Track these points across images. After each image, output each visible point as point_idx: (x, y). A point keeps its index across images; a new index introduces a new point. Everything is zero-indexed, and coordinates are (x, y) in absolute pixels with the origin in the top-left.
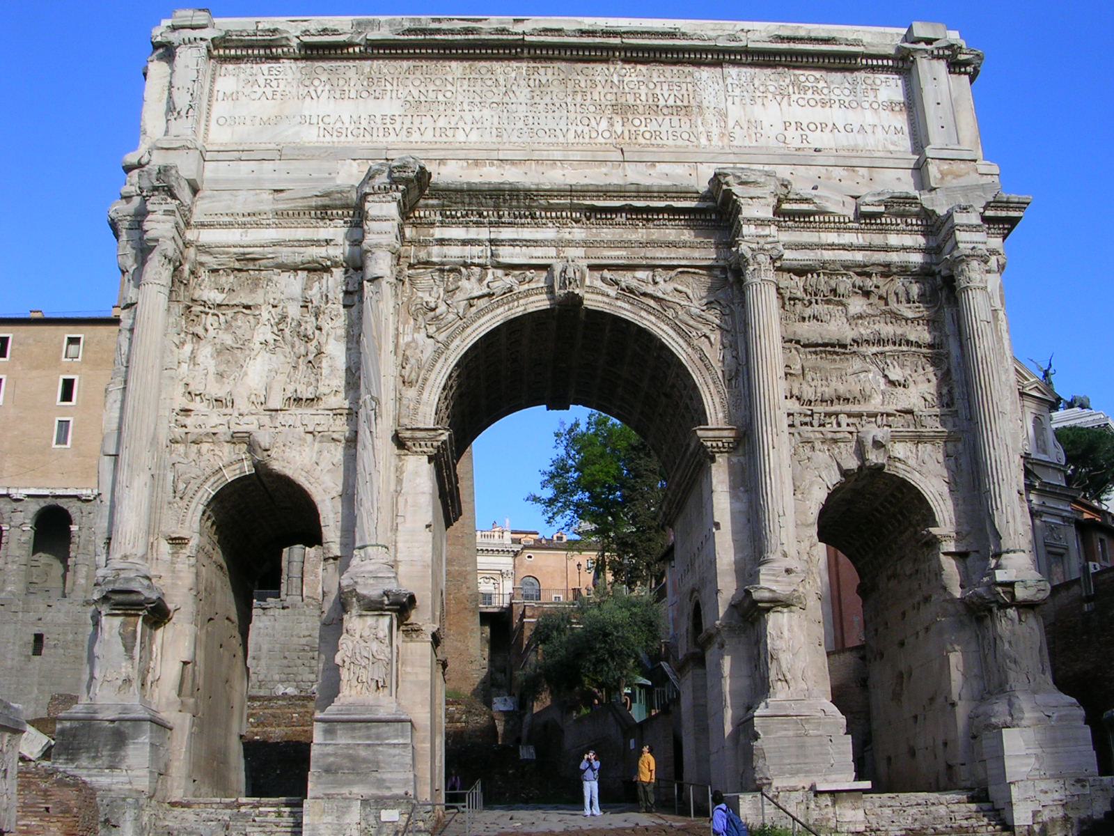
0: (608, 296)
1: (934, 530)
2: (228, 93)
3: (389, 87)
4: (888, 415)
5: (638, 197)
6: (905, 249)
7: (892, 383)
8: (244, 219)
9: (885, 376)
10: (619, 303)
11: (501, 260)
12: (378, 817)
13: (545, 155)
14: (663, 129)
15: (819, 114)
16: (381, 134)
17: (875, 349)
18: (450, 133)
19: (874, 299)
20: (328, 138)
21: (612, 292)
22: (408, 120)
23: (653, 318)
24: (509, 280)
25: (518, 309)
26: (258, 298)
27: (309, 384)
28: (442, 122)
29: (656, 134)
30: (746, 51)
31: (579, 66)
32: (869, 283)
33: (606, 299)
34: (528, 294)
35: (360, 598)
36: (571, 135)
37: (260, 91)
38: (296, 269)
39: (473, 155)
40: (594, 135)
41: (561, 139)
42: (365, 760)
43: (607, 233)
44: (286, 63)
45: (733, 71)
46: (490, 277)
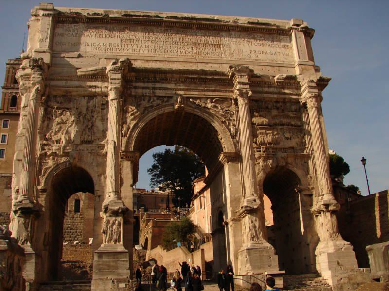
0: (192, 107)
2: (60, 33)
3: (116, 34)
4: (285, 149)
5: (202, 75)
7: (287, 138)
8: (67, 78)
9: (284, 136)
10: (196, 110)
11: (156, 94)
12: (118, 286)
13: (171, 59)
14: (210, 51)
15: (262, 48)
16: (114, 50)
17: (280, 127)
20: (95, 51)
21: (193, 106)
22: (123, 46)
23: (207, 115)
24: (159, 102)
25: (161, 112)
26: (71, 105)
27: (89, 136)
28: (135, 47)
29: (207, 53)
30: (238, 27)
31: (182, 30)
32: (278, 105)
33: (191, 108)
34: (165, 106)
35: (111, 209)
36: (179, 53)
38: (84, 96)
40: (187, 53)
42: (113, 266)
44: (81, 25)
46: (152, 100)
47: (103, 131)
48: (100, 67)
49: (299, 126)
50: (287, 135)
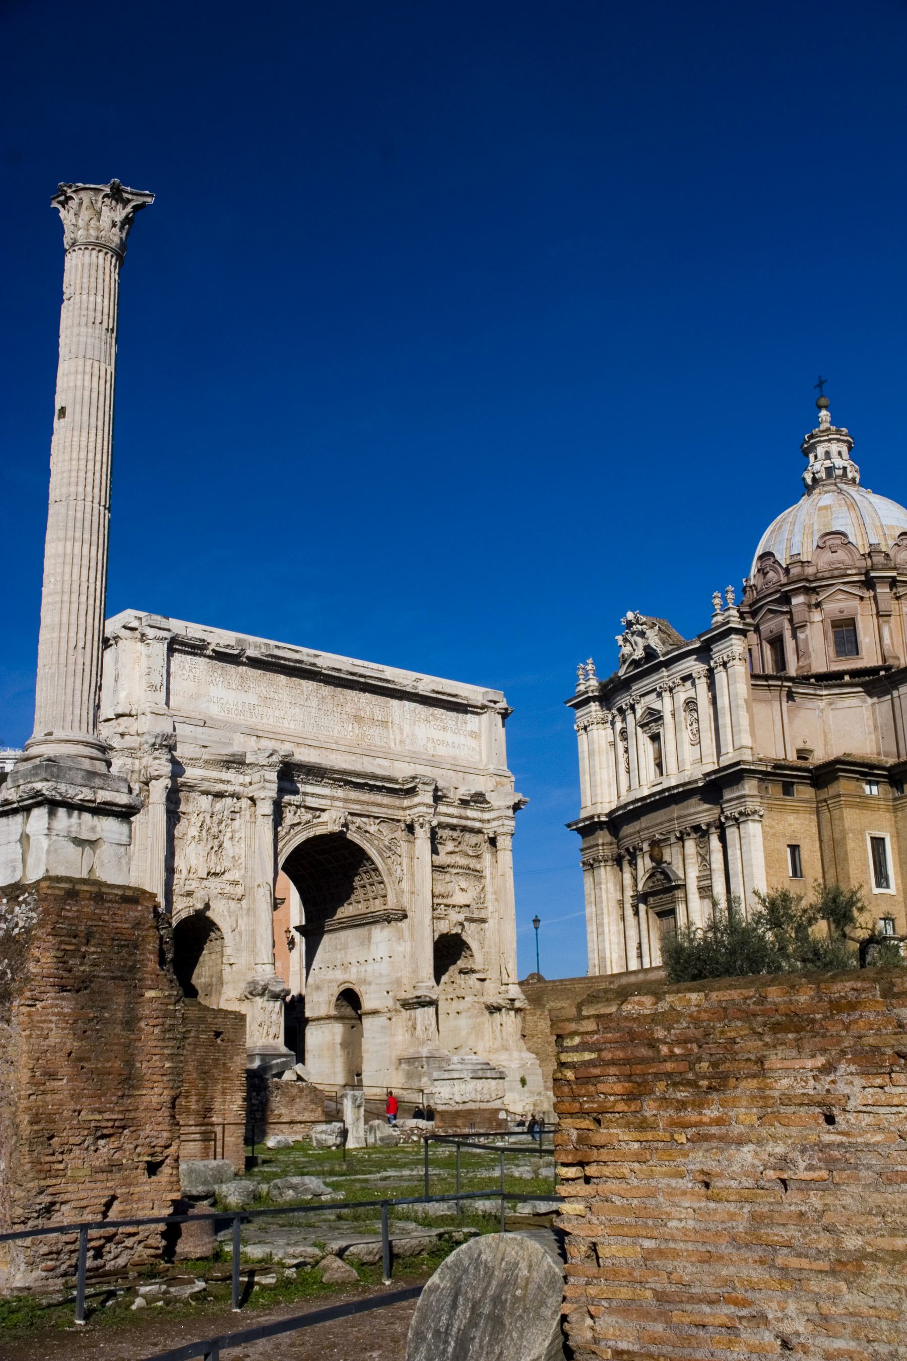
1: (476, 968)
4: (461, 907)
6: (474, 819)
7: (462, 890)
10: (355, 835)
11: (308, 804)
13: (329, 746)
18: (281, 720)
19: (456, 843)
20: (223, 714)
24: (308, 816)
30: (417, 695)
31: (340, 689)
32: (455, 834)
35: (271, 991)
36: (336, 732)
37: (187, 674)
39: (297, 740)
41: (331, 734)
43: (354, 794)
45: (406, 703)
47: (234, 857)
48: (236, 748)
49: (478, 871)
50: (464, 885)
